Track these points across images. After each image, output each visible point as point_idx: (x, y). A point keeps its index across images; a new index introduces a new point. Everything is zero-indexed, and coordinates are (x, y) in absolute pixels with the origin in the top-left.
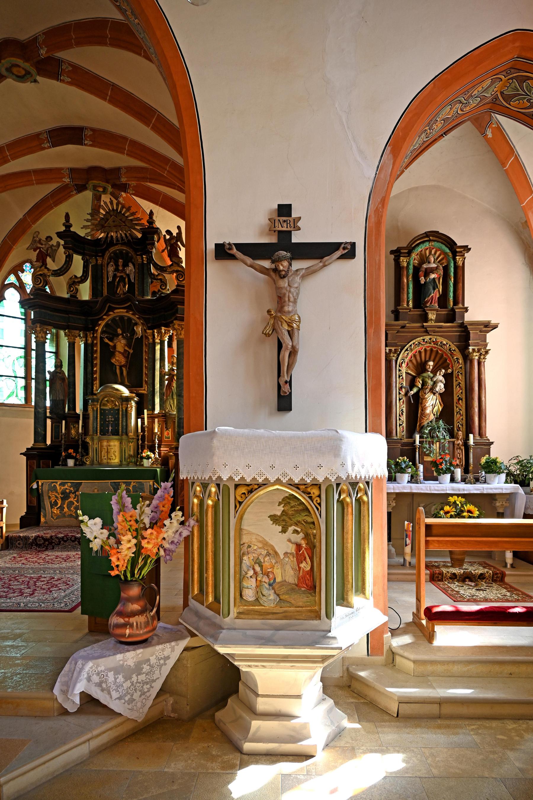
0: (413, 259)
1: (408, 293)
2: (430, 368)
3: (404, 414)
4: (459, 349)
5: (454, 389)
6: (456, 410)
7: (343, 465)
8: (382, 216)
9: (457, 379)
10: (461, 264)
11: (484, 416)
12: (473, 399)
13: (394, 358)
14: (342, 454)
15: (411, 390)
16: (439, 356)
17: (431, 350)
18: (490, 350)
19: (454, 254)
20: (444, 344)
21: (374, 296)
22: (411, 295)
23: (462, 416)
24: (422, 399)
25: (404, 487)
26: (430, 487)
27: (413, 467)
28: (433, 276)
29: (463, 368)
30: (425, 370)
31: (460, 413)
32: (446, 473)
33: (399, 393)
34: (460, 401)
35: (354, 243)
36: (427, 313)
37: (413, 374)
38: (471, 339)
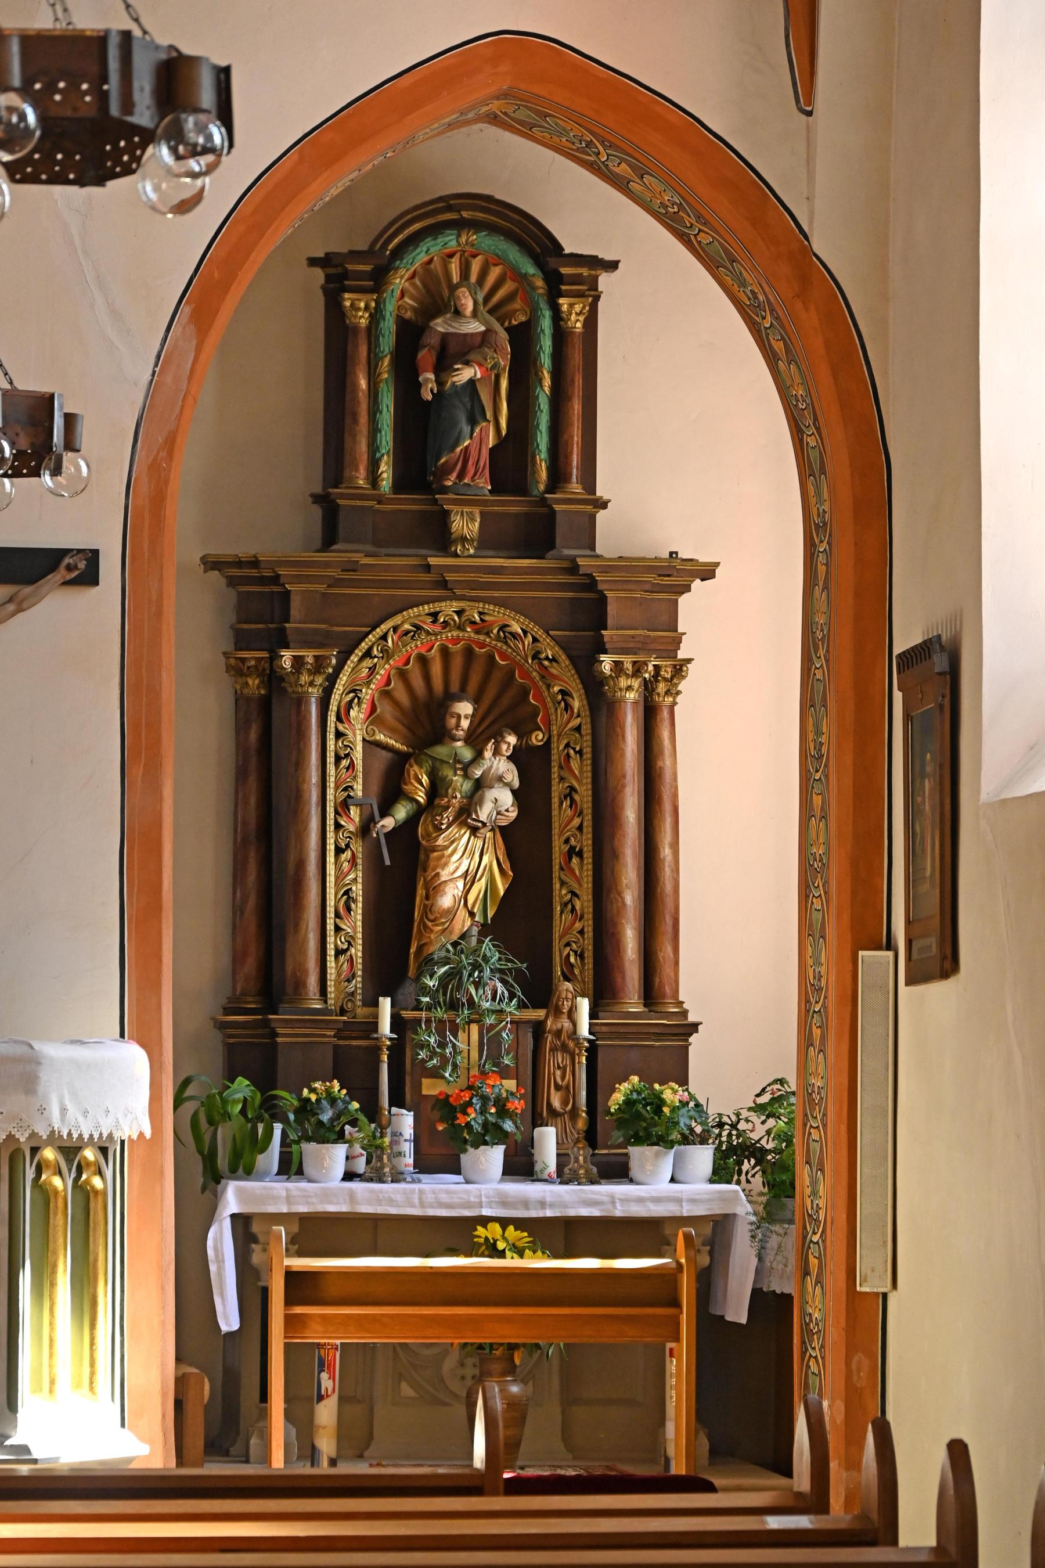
0: (397, 293)
1: (374, 430)
2: (458, 725)
3: (358, 909)
4: (570, 658)
5: (555, 813)
6: (560, 893)
7: (42, 1110)
8: (167, 482)
9: (562, 773)
10: (579, 325)
11: (669, 920)
12: (616, 856)
13: (315, 693)
14: (41, 1089)
15: (385, 811)
16: (497, 677)
17: (469, 653)
18: (689, 661)
19: (555, 285)
20: (514, 635)
21: (145, 682)
22: (386, 439)
23: (582, 918)
24: (425, 849)
25: (327, 1195)
26: (421, 1191)
27: (362, 1118)
28: (465, 374)
29: (586, 729)
30: (441, 734)
31: (573, 909)
32: (486, 1143)
33: (338, 826)
34: (575, 860)
35: (95, 553)
36: (446, 514)
37: (398, 745)
38: (610, 622)
